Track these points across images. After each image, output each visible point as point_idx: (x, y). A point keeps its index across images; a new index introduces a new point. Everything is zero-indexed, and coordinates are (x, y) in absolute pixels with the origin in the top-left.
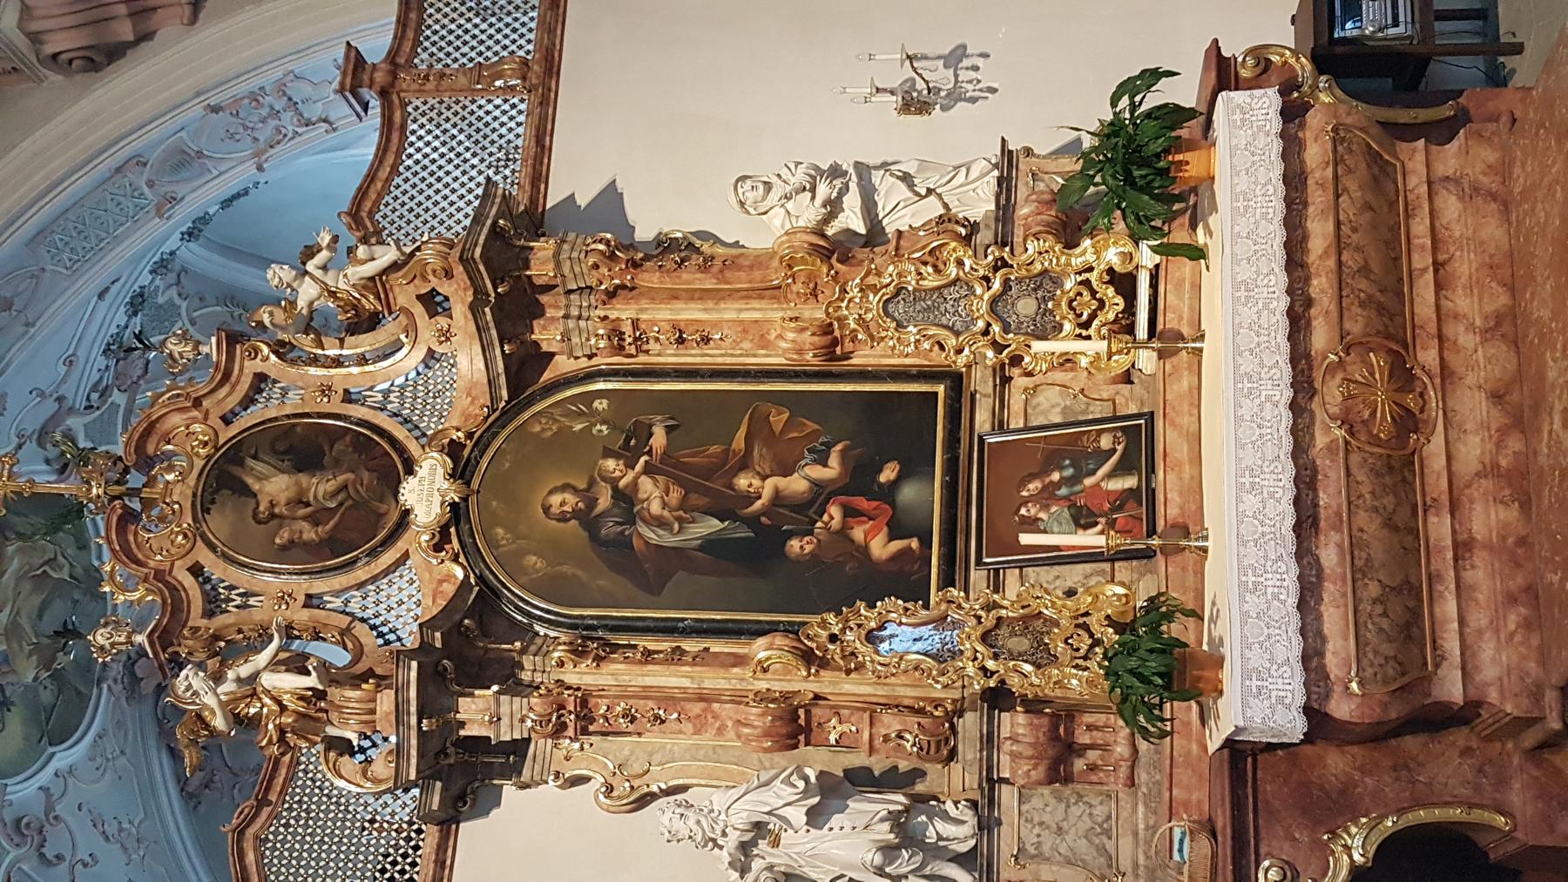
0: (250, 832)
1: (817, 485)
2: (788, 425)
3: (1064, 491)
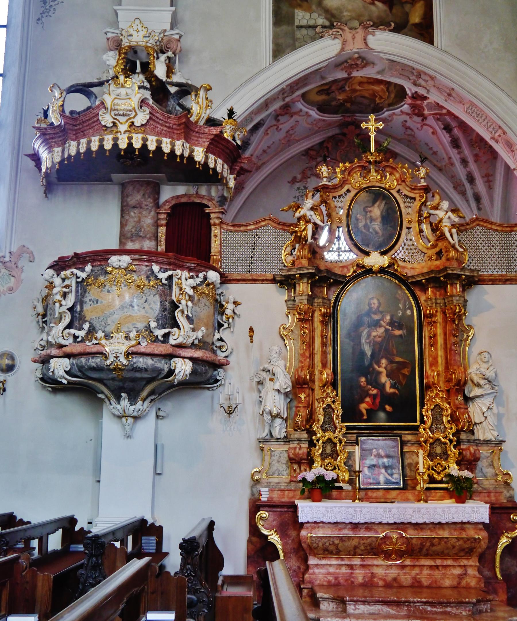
0: (270, 222)
1: (384, 385)
2: (404, 375)
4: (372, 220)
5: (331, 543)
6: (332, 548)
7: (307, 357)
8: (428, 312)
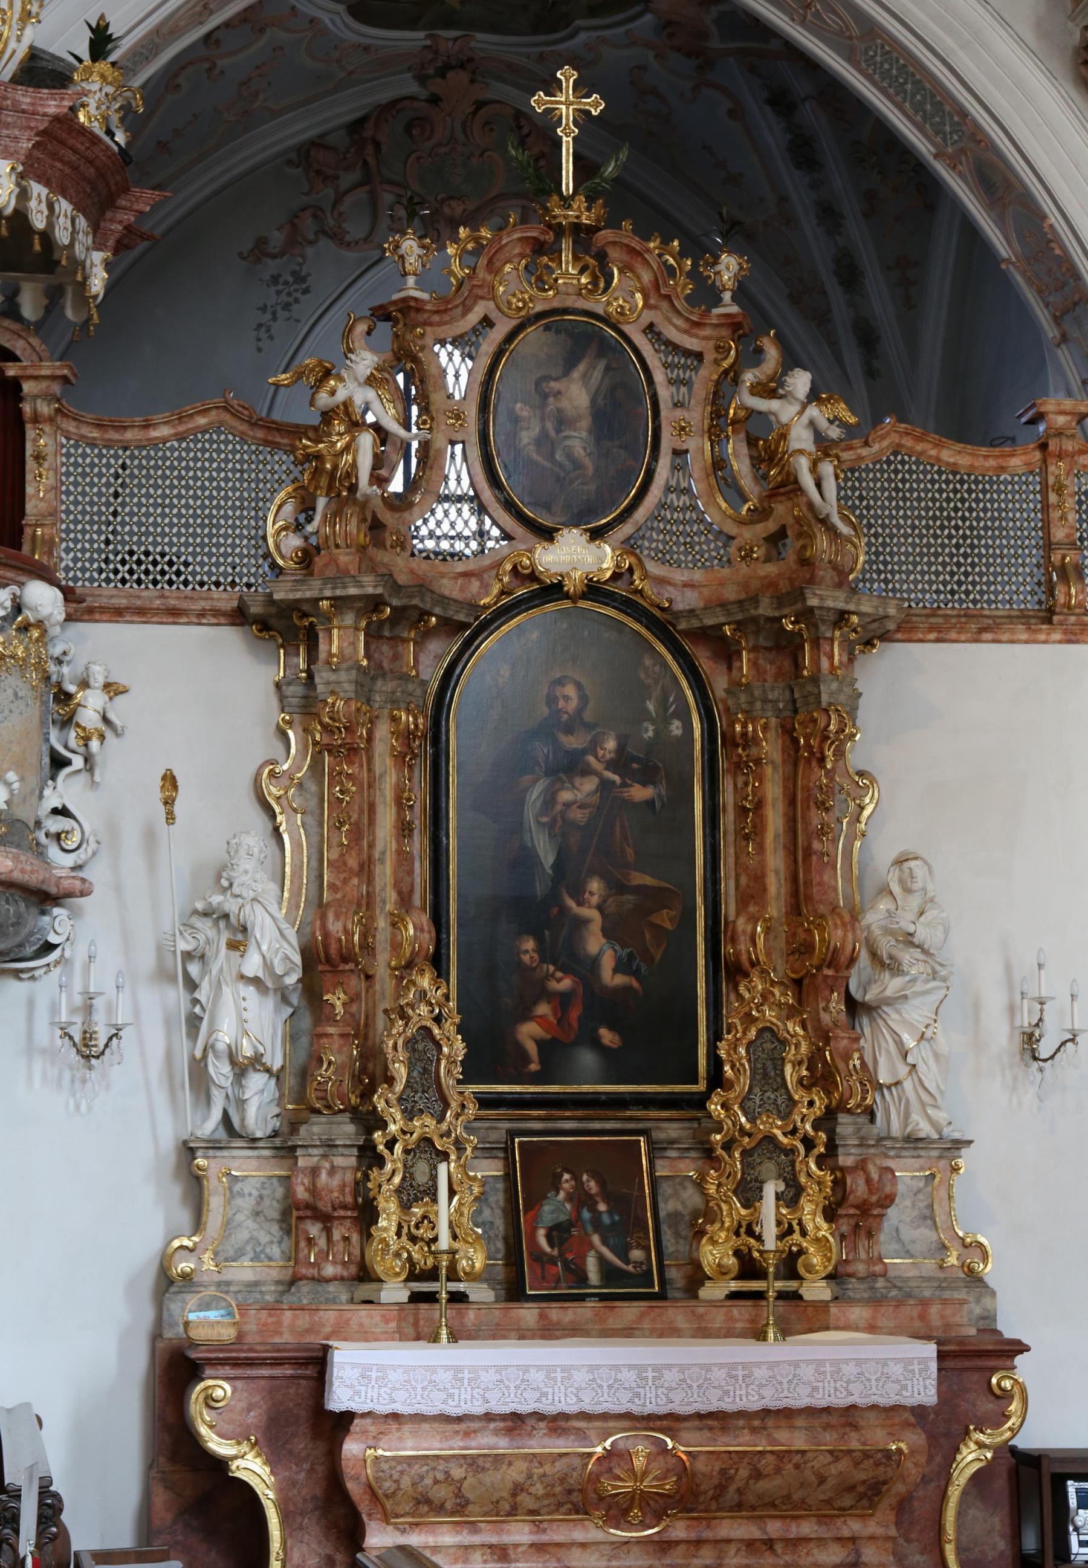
0: (227, 417)
1: (595, 963)
2: (658, 929)
3: (586, 1214)
4: (562, 421)
5: (440, 1476)
6: (442, 1493)
7: (351, 869)
8: (738, 728)
